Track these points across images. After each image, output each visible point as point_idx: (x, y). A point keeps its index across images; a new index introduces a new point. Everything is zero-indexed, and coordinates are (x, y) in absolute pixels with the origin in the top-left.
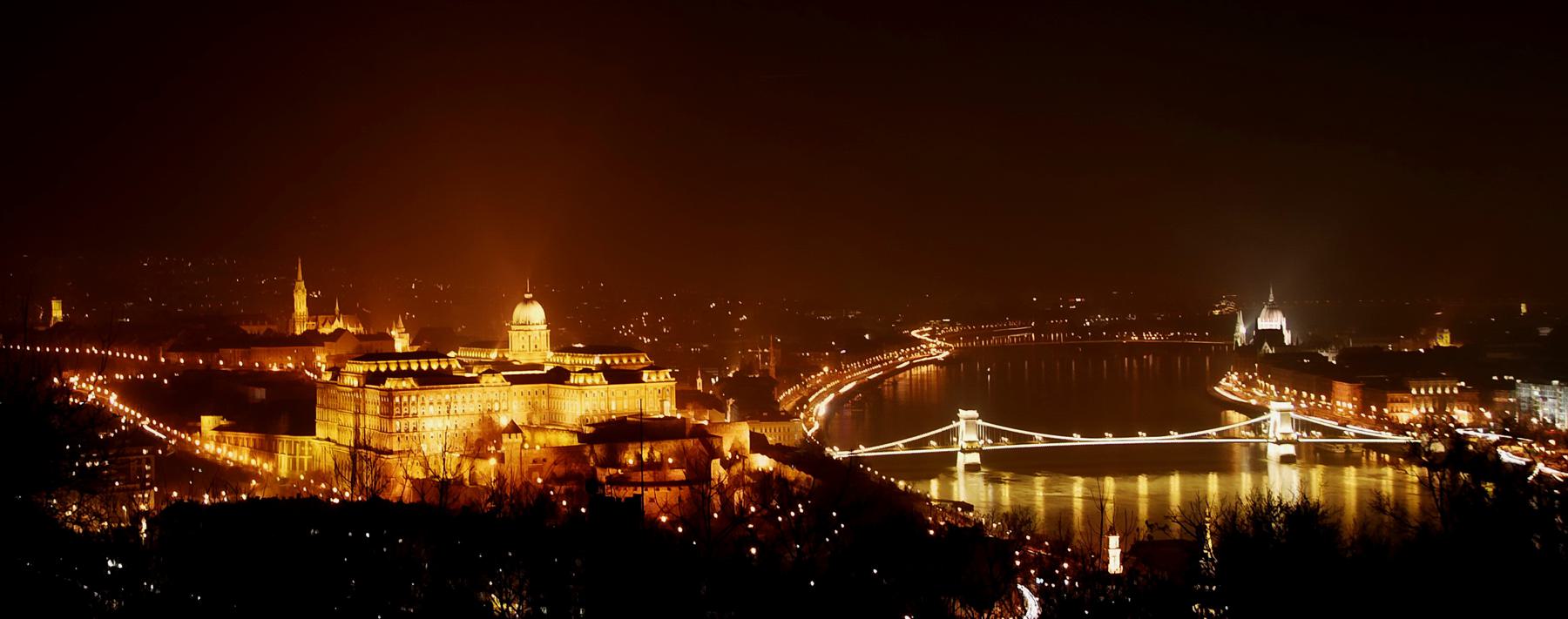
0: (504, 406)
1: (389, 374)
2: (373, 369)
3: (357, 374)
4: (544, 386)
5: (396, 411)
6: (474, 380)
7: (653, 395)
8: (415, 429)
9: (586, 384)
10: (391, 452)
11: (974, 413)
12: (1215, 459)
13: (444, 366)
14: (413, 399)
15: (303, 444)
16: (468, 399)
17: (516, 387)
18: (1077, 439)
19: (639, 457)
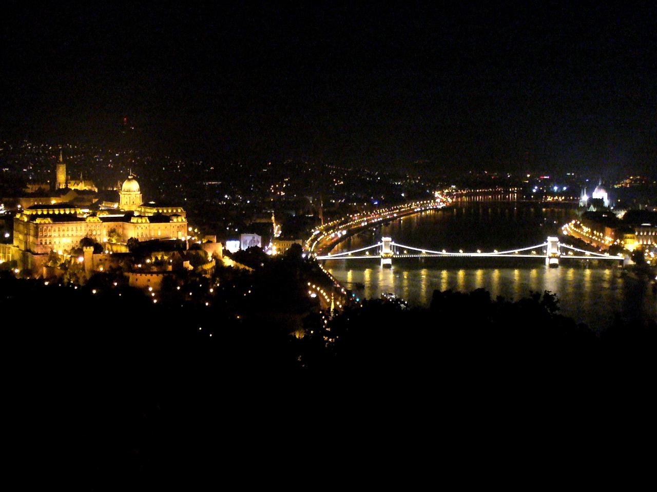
0: (99, 233)
1: (37, 216)
2: (34, 213)
3: (27, 216)
4: (121, 223)
5: (40, 234)
6: (83, 220)
7: (178, 229)
8: (50, 243)
9: (137, 223)
10: (37, 254)
11: (389, 239)
12: (526, 264)
13: (73, 212)
14: (49, 228)
15: (9, 248)
16: (79, 229)
17: (105, 224)
18: (444, 253)
19: (157, 258)
